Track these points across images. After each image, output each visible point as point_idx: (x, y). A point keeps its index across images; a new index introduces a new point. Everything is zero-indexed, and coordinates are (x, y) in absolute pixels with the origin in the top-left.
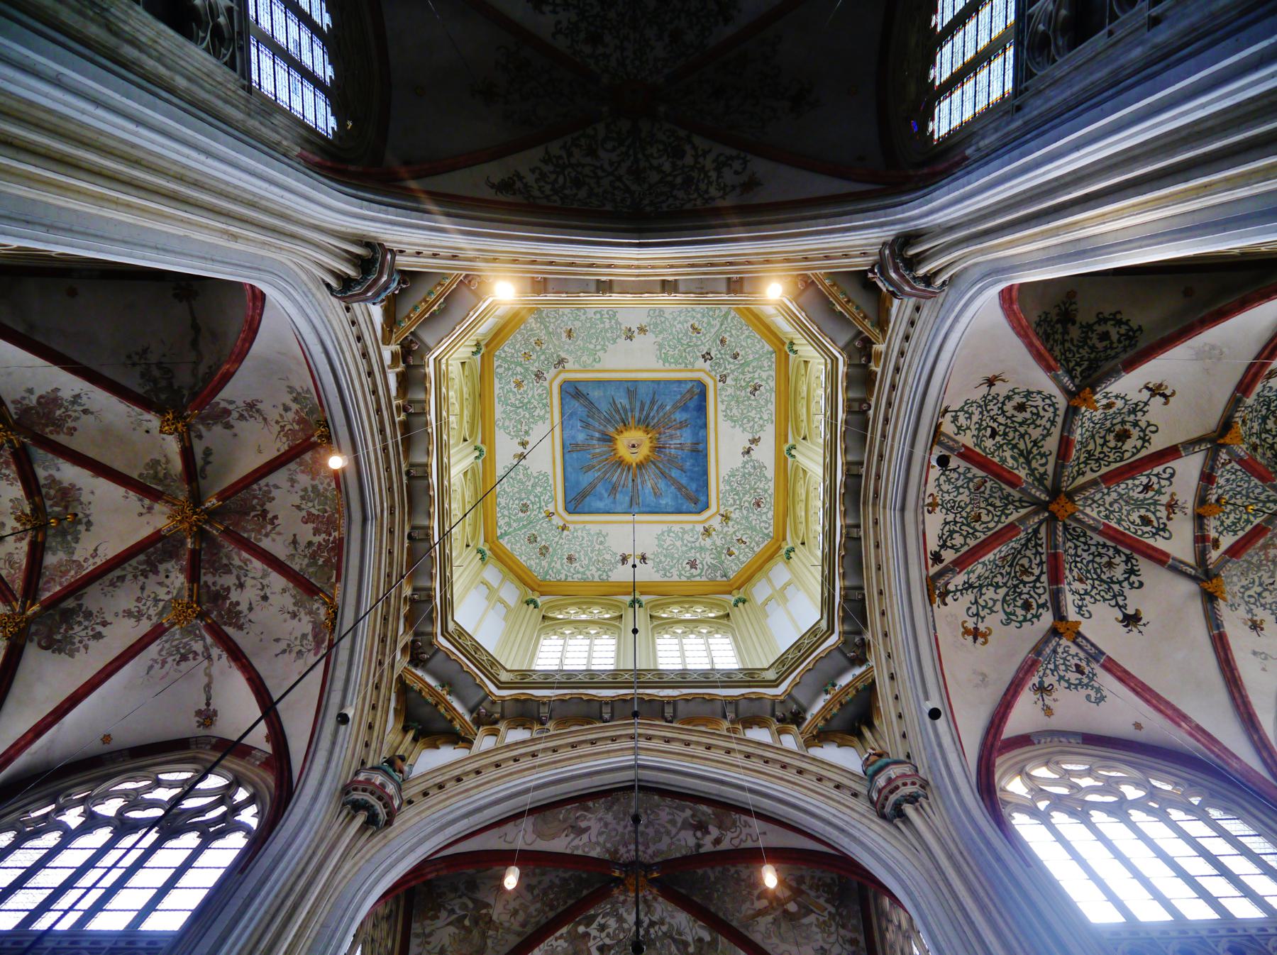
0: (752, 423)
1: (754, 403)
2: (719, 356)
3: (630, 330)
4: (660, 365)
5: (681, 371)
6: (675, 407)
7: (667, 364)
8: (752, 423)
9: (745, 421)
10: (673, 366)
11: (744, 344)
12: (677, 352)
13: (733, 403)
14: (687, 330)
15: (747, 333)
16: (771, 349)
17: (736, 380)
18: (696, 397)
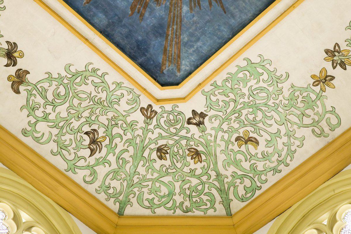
0: (50, 97)
1: (76, 124)
2: (183, 133)
3: (343, 65)
4: (252, 54)
5: (216, 71)
6: (178, 19)
7: (244, 64)
8: (50, 97)
9: (62, 90)
10: (232, 68)
11: (166, 179)
12: (245, 91)
13: (103, 96)
14: (257, 130)
15: (178, 199)
16: (128, 211)
17: (132, 125)
18: (161, 59)
